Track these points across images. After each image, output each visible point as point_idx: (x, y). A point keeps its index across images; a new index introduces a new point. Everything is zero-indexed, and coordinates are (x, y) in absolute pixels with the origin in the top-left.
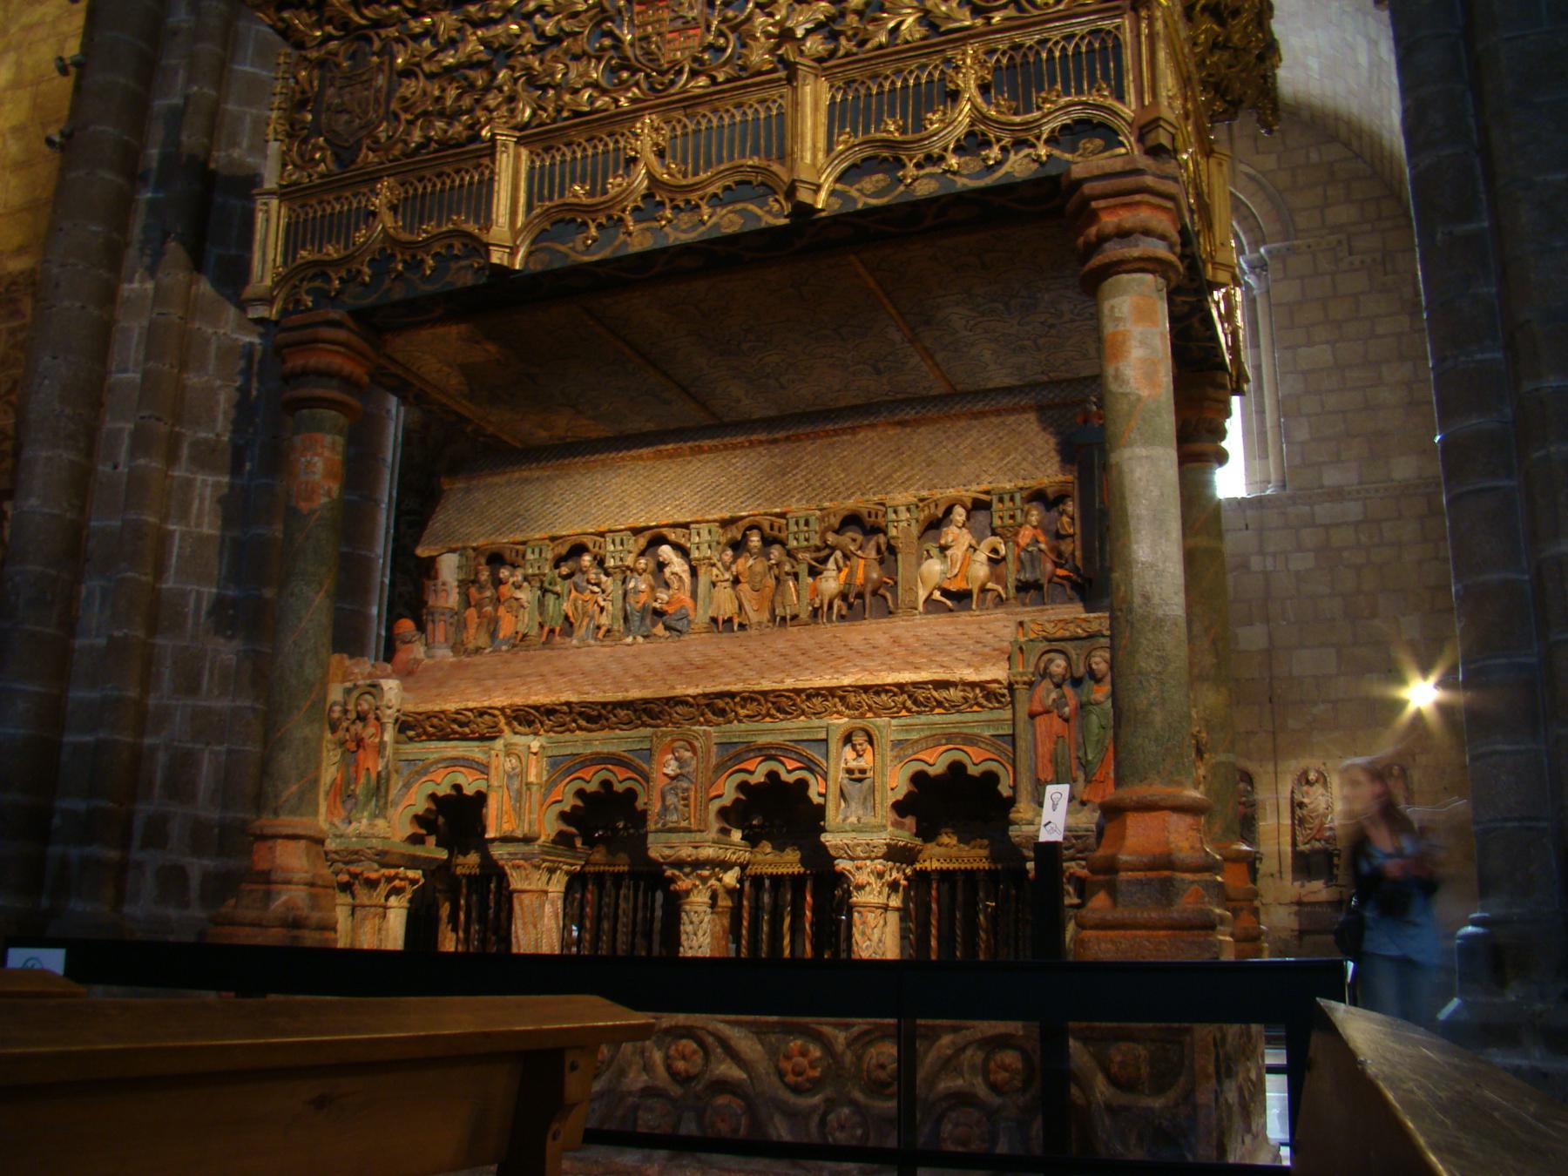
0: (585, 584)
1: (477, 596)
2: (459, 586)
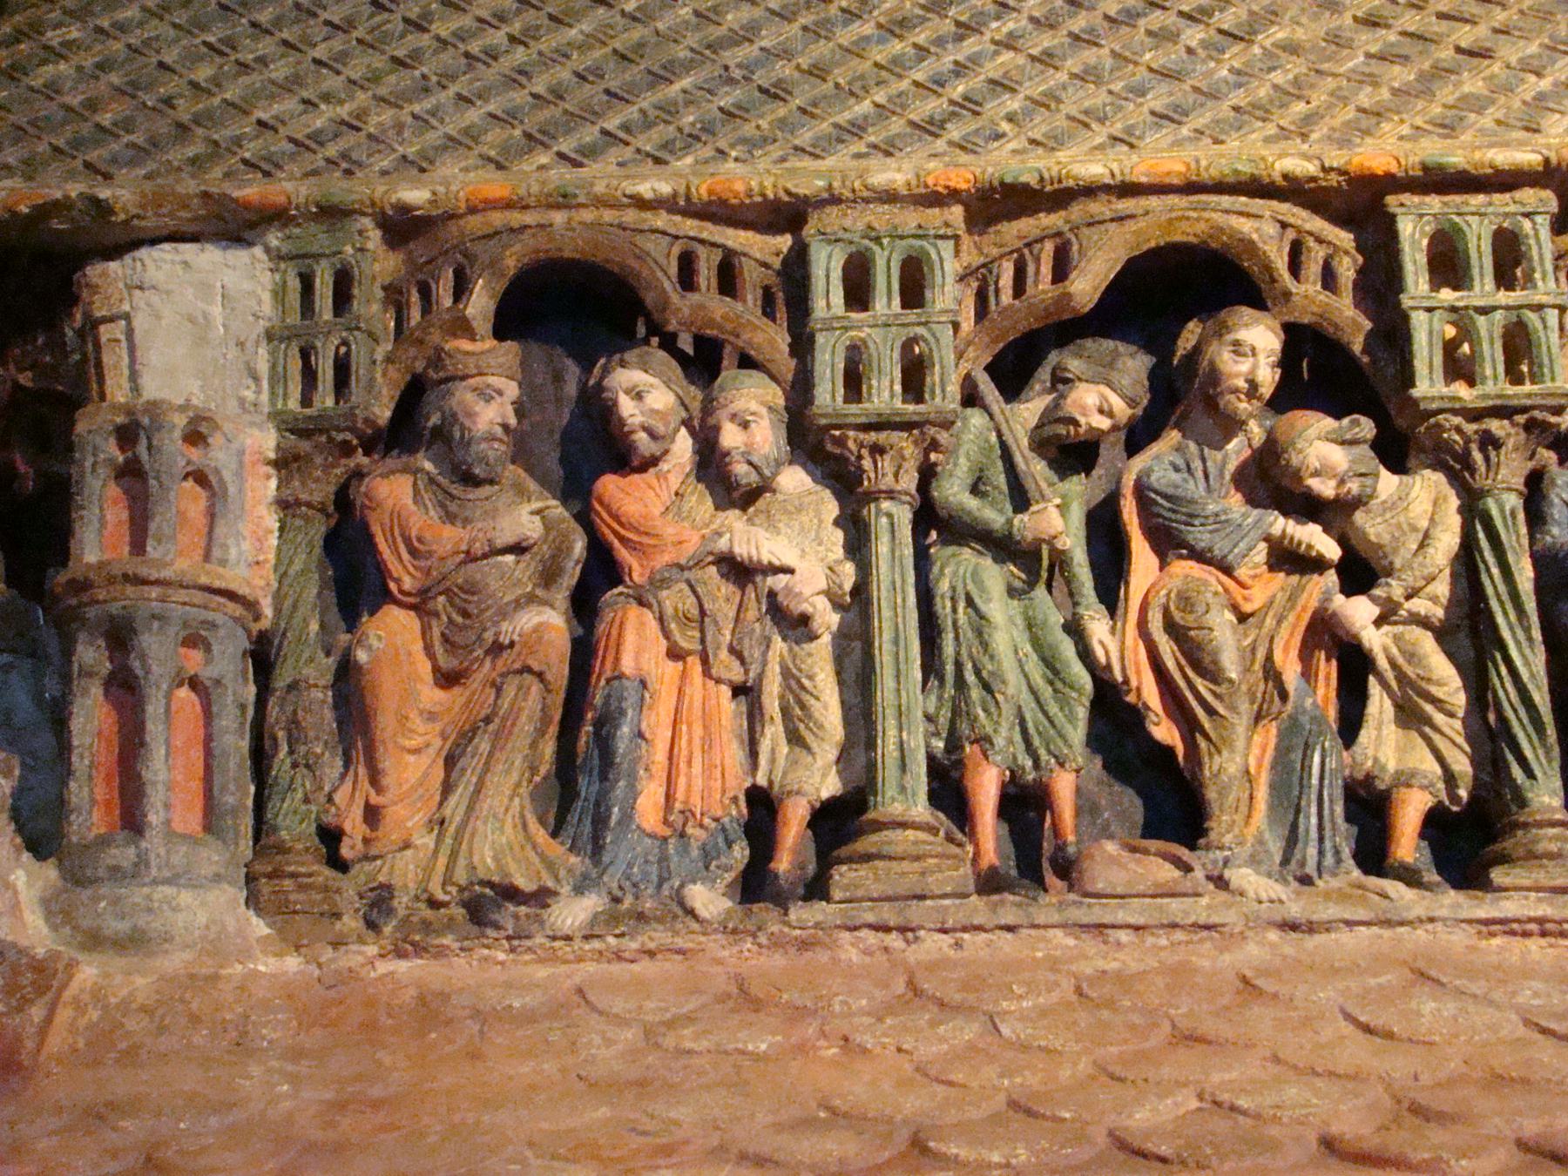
0: (1235, 503)
1: (449, 538)
2: (284, 463)
